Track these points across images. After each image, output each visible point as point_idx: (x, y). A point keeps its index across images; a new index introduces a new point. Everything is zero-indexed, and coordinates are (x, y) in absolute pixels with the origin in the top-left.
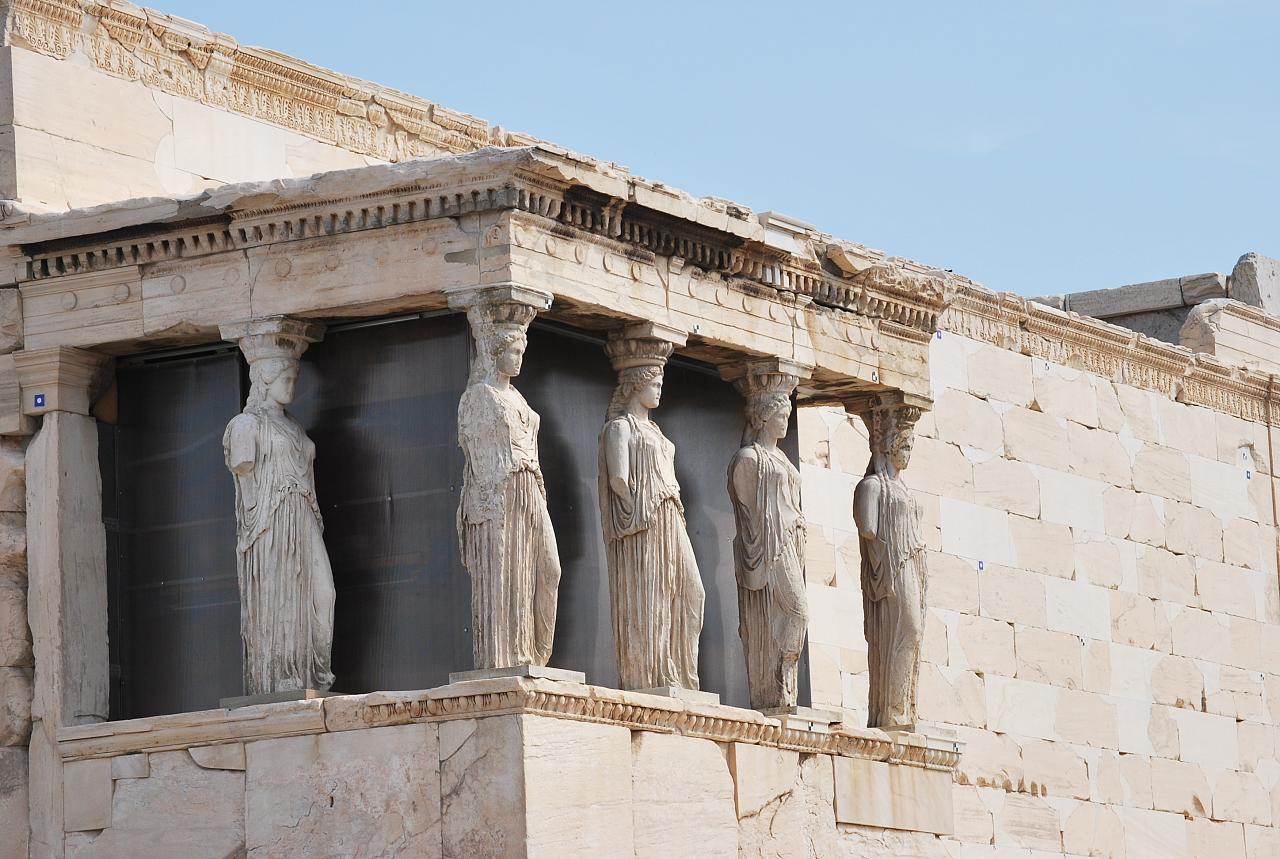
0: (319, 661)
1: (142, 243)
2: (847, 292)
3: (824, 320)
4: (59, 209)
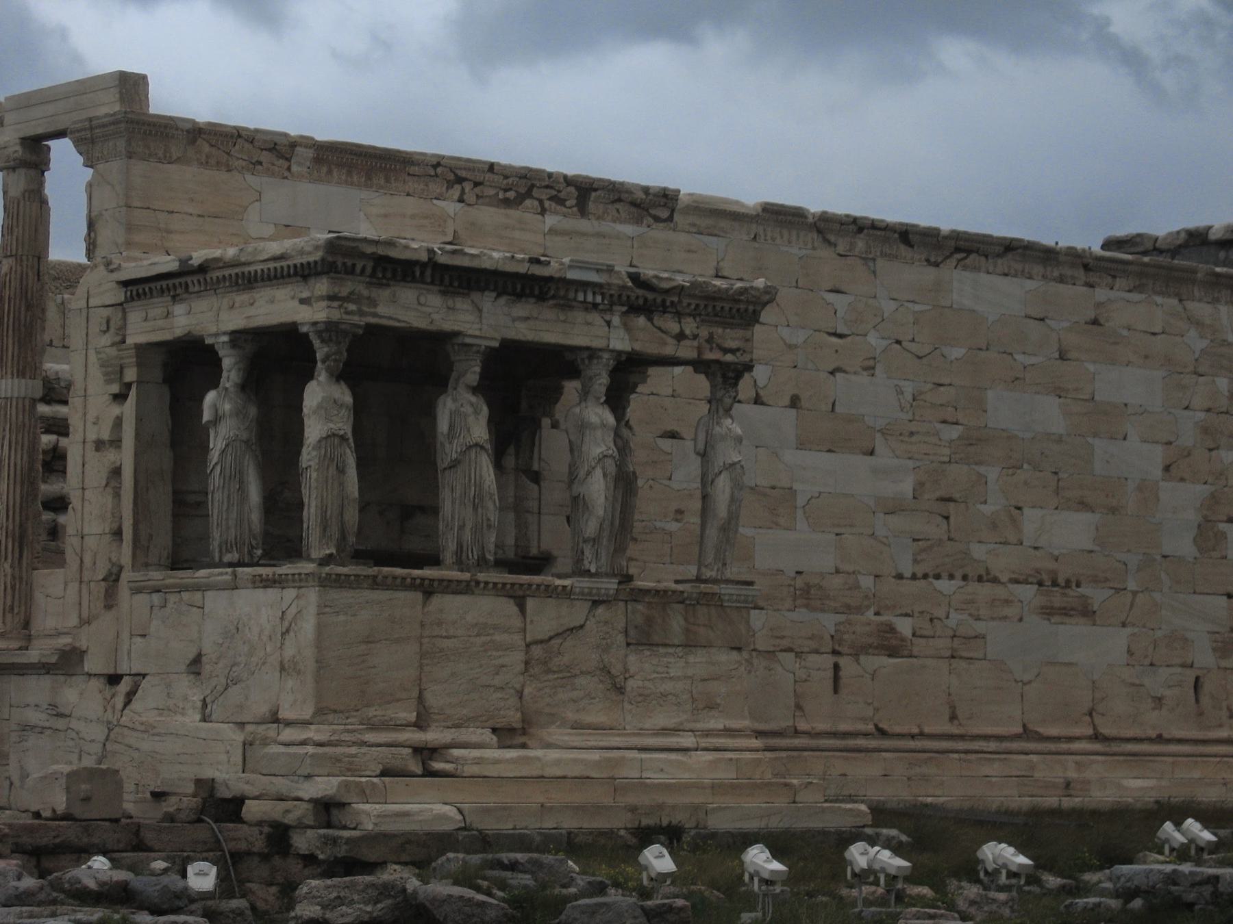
0: (254, 542)
1: (170, 282)
2: (664, 301)
3: (641, 320)
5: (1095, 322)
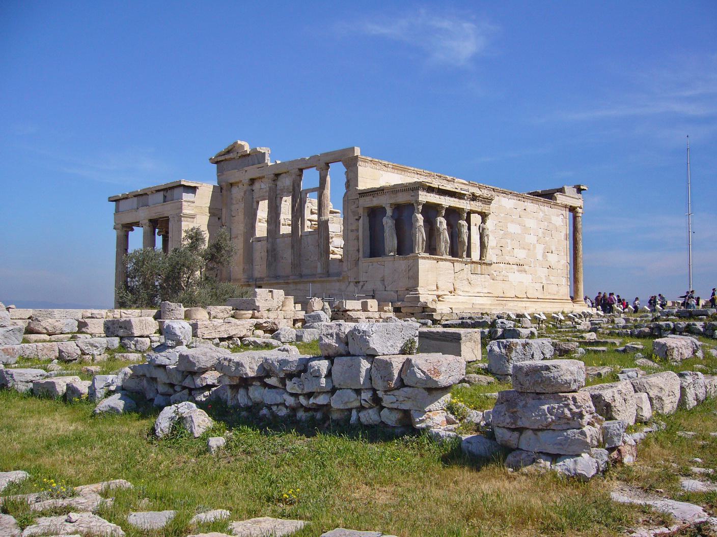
3: (472, 202)
4: (363, 188)
5: (525, 210)
